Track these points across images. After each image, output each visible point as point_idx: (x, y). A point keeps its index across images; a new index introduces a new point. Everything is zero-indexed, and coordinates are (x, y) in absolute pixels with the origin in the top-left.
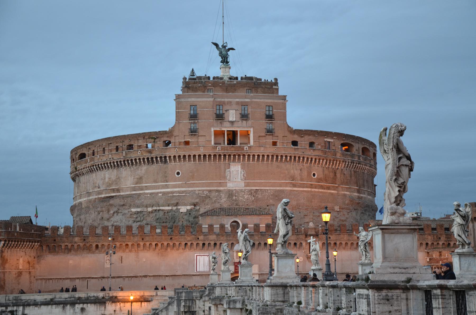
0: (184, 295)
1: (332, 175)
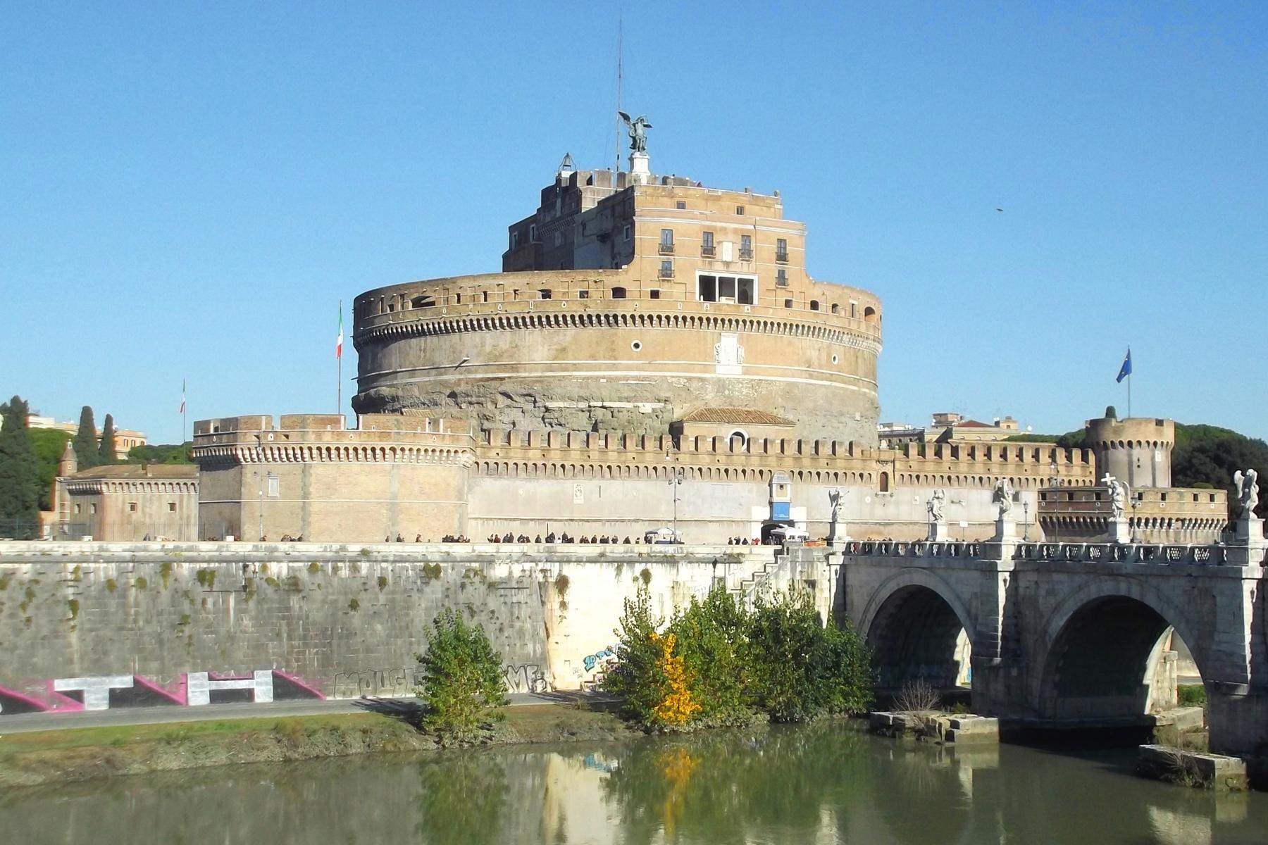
0: (800, 554)
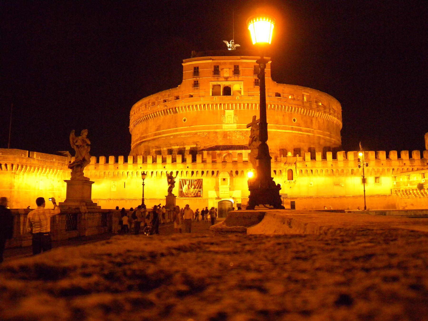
1: (309, 121)
